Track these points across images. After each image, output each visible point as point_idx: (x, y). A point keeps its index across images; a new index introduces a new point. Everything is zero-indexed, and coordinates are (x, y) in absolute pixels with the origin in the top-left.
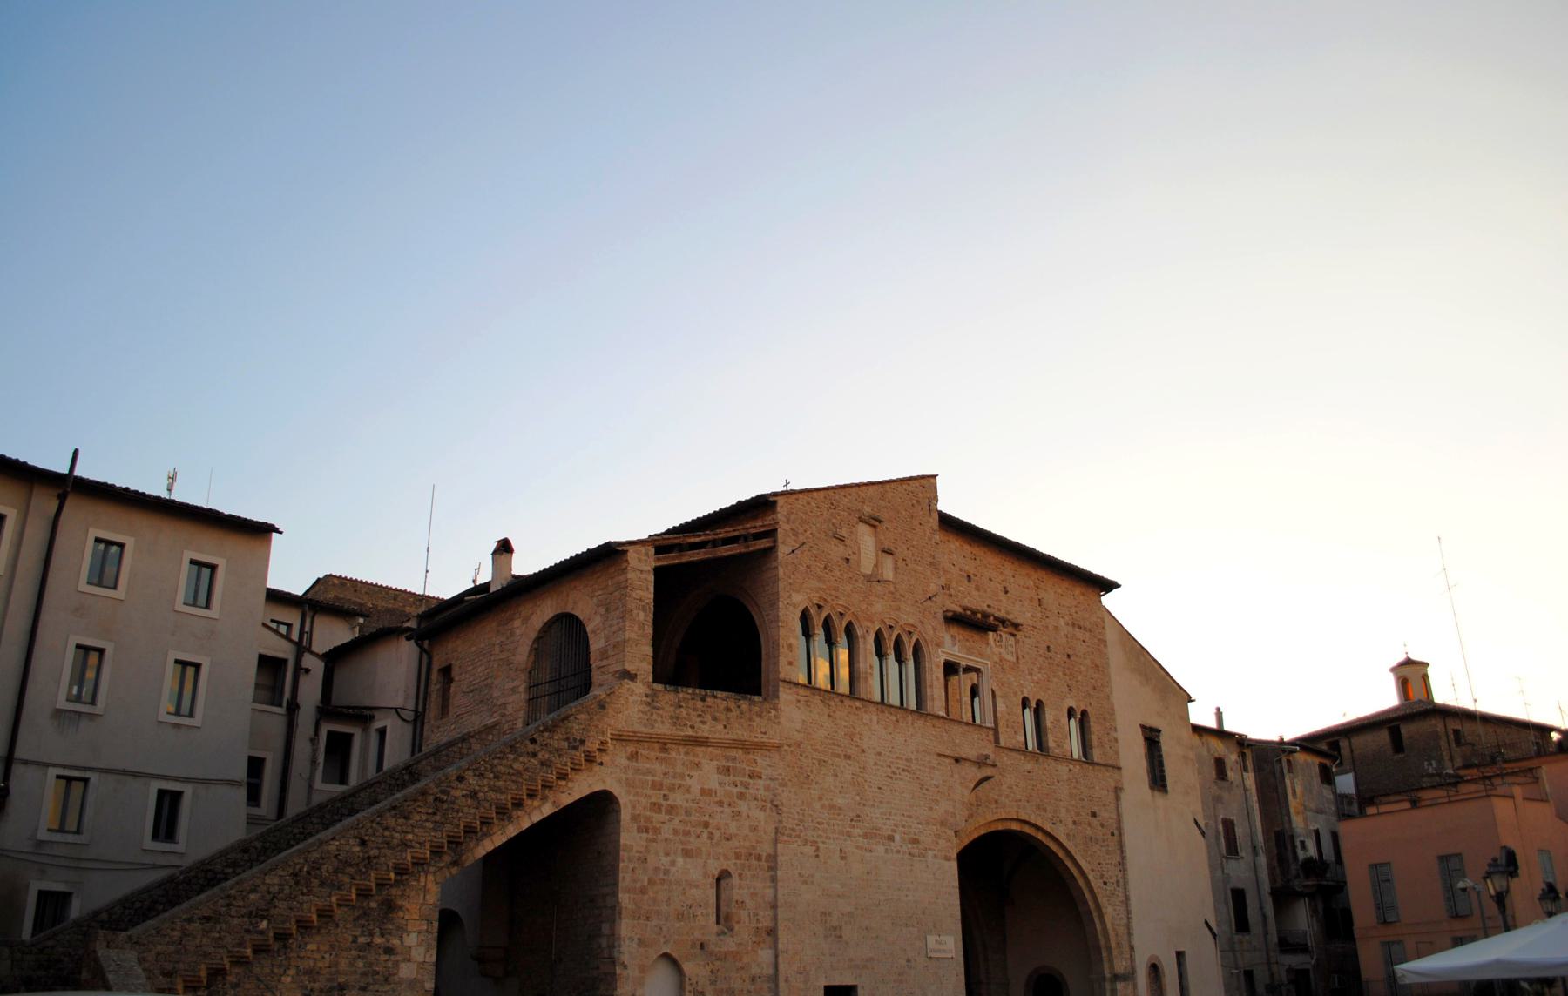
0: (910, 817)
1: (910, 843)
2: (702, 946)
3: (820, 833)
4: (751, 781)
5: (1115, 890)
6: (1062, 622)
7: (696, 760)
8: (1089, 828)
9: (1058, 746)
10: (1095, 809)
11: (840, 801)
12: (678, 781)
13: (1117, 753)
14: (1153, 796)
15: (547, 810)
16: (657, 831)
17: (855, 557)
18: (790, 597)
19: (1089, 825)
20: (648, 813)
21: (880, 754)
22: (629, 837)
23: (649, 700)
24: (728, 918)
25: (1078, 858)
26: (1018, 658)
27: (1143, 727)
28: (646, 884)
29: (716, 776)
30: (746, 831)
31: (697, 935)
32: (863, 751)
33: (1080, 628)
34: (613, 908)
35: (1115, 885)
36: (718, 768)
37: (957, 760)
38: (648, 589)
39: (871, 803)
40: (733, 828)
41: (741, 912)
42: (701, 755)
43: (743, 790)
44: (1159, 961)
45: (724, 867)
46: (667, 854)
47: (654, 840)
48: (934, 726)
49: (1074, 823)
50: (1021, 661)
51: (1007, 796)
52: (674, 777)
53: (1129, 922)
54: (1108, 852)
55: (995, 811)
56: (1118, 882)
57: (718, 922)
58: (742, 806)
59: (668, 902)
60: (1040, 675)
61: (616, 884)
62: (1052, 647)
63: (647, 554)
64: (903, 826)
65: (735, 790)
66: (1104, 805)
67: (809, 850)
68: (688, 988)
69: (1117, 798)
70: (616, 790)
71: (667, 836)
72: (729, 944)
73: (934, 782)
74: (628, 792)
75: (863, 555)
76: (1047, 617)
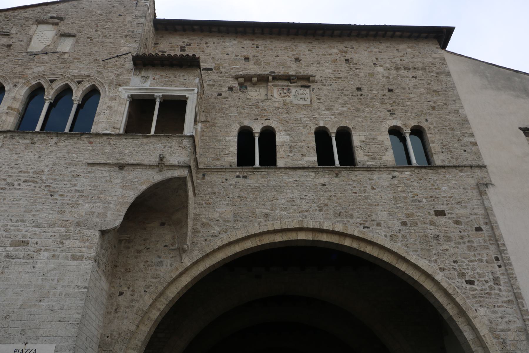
5: (491, 288)
8: (432, 227)
9: (374, 159)
10: (440, 208)
19: (432, 223)
25: (413, 258)
35: (491, 283)
37: (121, 167)
48: (91, 143)
49: (404, 224)
50: (316, 101)
51: (286, 209)
54: (471, 248)
55: (262, 224)
56: (496, 281)
60: (345, 109)
66: (459, 203)
69: (482, 193)
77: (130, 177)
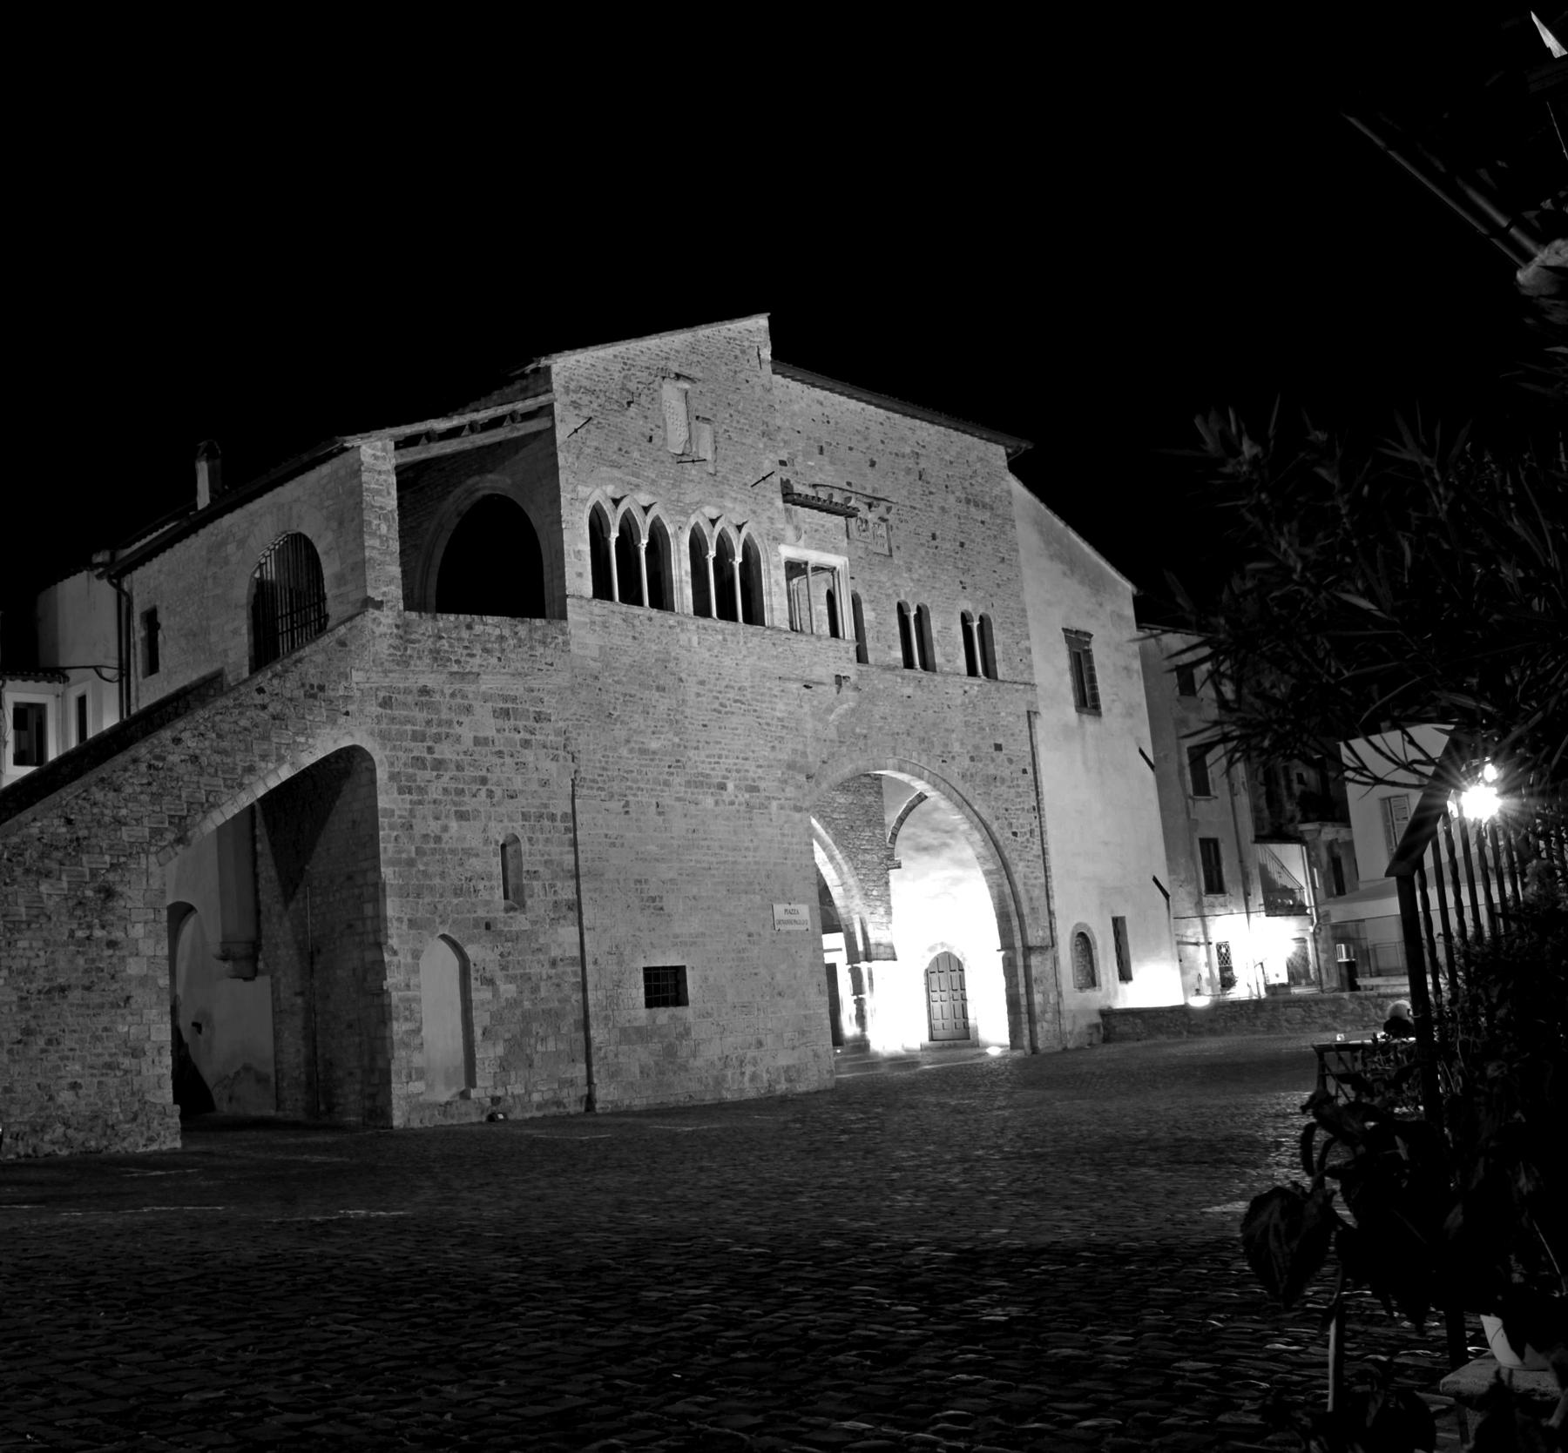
0: (746, 759)
1: (747, 791)
2: (488, 926)
3: (629, 783)
4: (538, 726)
6: (952, 499)
7: (466, 702)
9: (949, 661)
11: (654, 745)
12: (444, 730)
13: (1030, 666)
14: (1080, 721)
15: (286, 773)
16: (422, 790)
17: (660, 432)
18: (574, 490)
19: (993, 760)
20: (410, 770)
21: (702, 683)
22: (387, 800)
23: (401, 632)
24: (519, 890)
26: (890, 550)
27: (1065, 630)
28: (413, 855)
29: (492, 721)
30: (534, 786)
31: (481, 913)
32: (681, 680)
33: (976, 505)
34: (376, 885)
36: (494, 711)
38: (389, 493)
39: (695, 744)
40: (518, 783)
41: (535, 883)
42: (470, 696)
43: (528, 736)
44: (1089, 929)
45: (510, 831)
46: (437, 818)
47: (420, 803)
49: (972, 759)
52: (439, 725)
53: (1047, 882)
56: (1032, 832)
57: (506, 897)
58: (529, 756)
59: (443, 875)
60: (921, 571)
61: (376, 856)
62: (938, 533)
63: (384, 449)
64: (738, 771)
65: (517, 737)
67: (616, 805)
68: (473, 974)
70: (368, 744)
71: (435, 796)
72: (521, 922)
73: (779, 714)
74: (383, 747)
75: (670, 427)
76: (931, 493)
77: (815, 703)
